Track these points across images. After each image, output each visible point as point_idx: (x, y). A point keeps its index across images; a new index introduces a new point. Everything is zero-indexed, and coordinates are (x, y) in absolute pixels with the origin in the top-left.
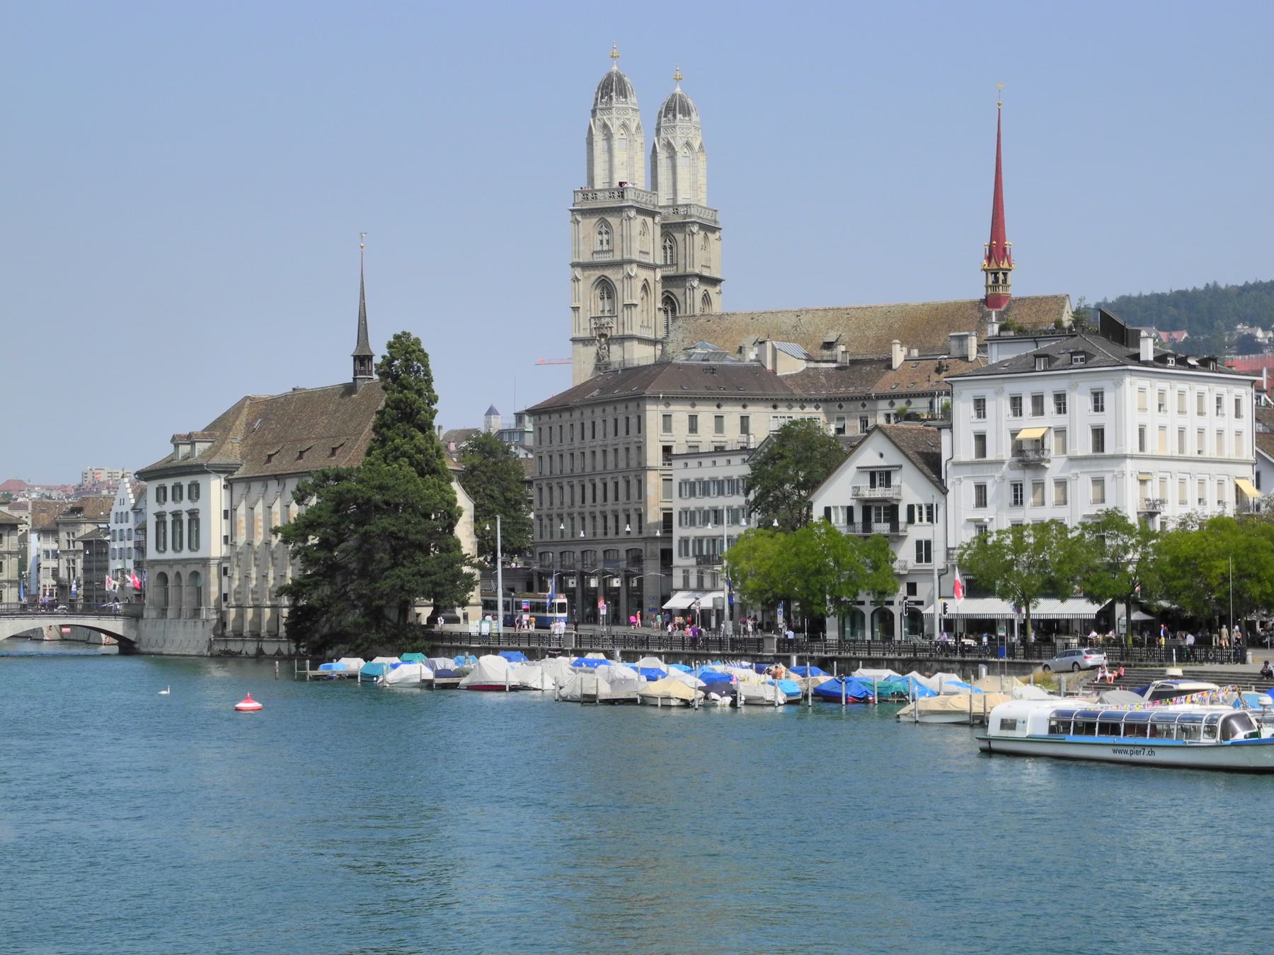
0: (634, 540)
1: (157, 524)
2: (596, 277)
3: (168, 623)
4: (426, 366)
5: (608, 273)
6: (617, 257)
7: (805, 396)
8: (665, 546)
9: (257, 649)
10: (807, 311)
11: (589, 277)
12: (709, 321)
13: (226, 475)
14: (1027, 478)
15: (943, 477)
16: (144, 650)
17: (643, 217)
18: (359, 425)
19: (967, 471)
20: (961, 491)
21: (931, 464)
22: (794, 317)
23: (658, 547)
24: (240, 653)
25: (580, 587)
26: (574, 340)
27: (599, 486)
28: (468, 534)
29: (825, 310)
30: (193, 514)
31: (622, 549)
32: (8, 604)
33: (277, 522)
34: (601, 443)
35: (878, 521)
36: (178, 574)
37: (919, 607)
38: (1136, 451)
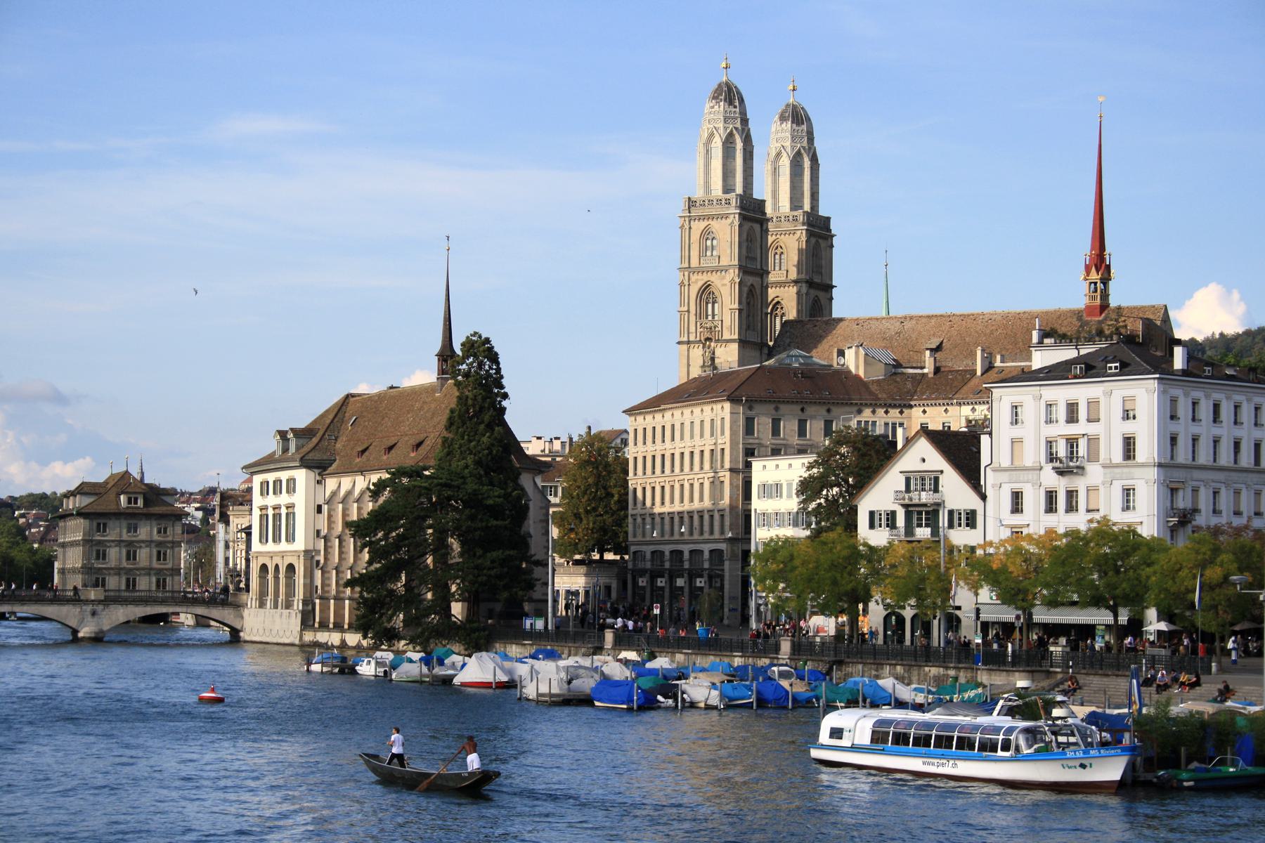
0: (716, 541)
1: (261, 516)
2: (700, 284)
3: (267, 613)
4: (498, 363)
5: (714, 278)
6: (725, 261)
7: (889, 402)
8: (745, 548)
9: (341, 640)
10: (911, 318)
11: (697, 281)
12: (816, 326)
13: (320, 470)
14: (1062, 485)
15: (982, 483)
16: (247, 638)
17: (750, 224)
18: (438, 423)
19: (1004, 477)
20: (999, 500)
21: (969, 468)
22: (898, 323)
23: (739, 549)
24: (327, 643)
25: (668, 586)
26: (679, 343)
27: (687, 486)
28: (543, 531)
29: (928, 317)
30: (290, 506)
31: (706, 548)
32: (173, 592)
33: (354, 517)
34: (689, 444)
35: (920, 525)
36: (277, 566)
37: (957, 612)
38: (1231, 464)
